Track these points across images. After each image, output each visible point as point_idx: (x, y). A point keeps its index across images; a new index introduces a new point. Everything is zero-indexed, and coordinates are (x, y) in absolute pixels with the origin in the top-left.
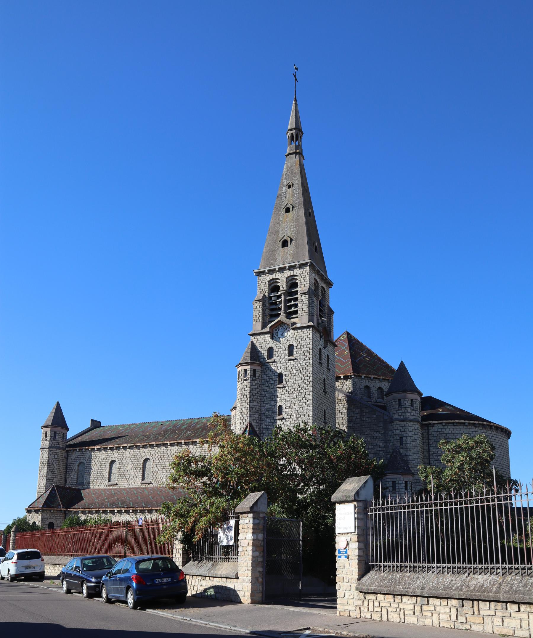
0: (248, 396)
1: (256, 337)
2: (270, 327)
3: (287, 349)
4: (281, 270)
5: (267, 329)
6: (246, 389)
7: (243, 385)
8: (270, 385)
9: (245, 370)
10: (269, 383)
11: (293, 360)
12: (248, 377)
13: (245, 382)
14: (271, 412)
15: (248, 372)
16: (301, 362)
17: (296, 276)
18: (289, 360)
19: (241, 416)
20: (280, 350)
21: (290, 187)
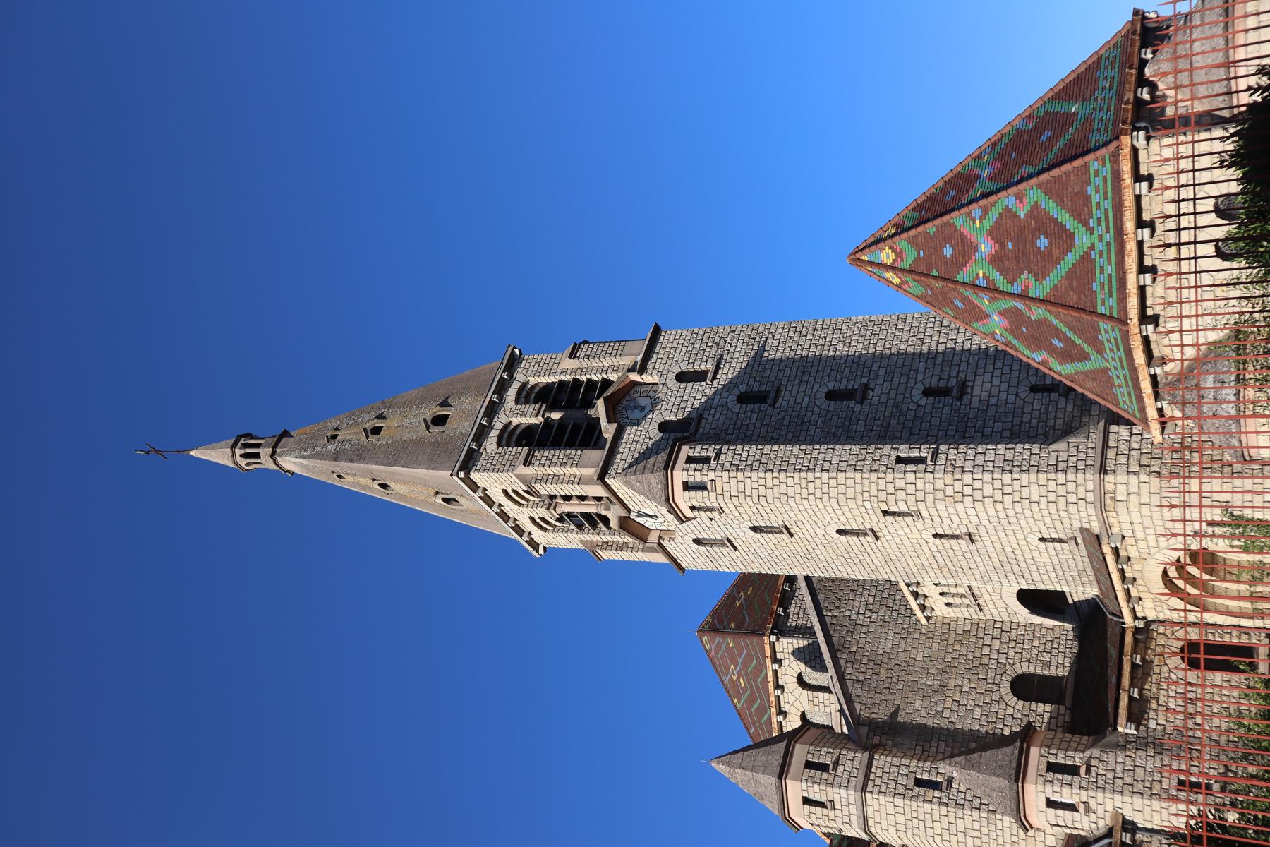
0: (767, 449)
1: (616, 465)
2: (609, 421)
3: (683, 385)
4: (492, 410)
5: (608, 430)
6: (745, 455)
7: (728, 464)
8: (758, 425)
9: (690, 460)
10: (751, 427)
11: (718, 368)
12: (710, 452)
13: (723, 457)
14: (835, 419)
15: (698, 451)
16: (732, 349)
17: (524, 385)
18: (714, 378)
19: (819, 468)
20: (678, 399)
21: (334, 437)
